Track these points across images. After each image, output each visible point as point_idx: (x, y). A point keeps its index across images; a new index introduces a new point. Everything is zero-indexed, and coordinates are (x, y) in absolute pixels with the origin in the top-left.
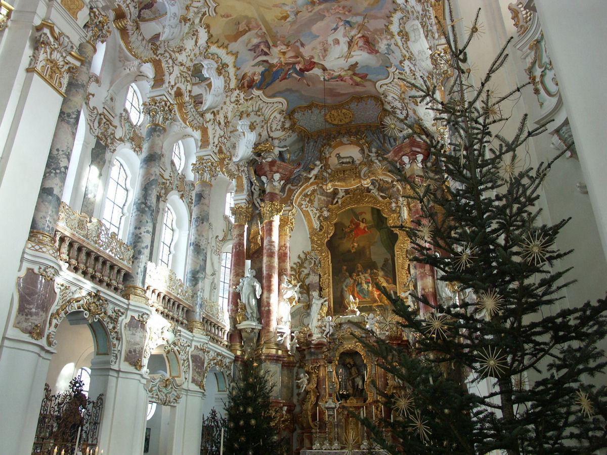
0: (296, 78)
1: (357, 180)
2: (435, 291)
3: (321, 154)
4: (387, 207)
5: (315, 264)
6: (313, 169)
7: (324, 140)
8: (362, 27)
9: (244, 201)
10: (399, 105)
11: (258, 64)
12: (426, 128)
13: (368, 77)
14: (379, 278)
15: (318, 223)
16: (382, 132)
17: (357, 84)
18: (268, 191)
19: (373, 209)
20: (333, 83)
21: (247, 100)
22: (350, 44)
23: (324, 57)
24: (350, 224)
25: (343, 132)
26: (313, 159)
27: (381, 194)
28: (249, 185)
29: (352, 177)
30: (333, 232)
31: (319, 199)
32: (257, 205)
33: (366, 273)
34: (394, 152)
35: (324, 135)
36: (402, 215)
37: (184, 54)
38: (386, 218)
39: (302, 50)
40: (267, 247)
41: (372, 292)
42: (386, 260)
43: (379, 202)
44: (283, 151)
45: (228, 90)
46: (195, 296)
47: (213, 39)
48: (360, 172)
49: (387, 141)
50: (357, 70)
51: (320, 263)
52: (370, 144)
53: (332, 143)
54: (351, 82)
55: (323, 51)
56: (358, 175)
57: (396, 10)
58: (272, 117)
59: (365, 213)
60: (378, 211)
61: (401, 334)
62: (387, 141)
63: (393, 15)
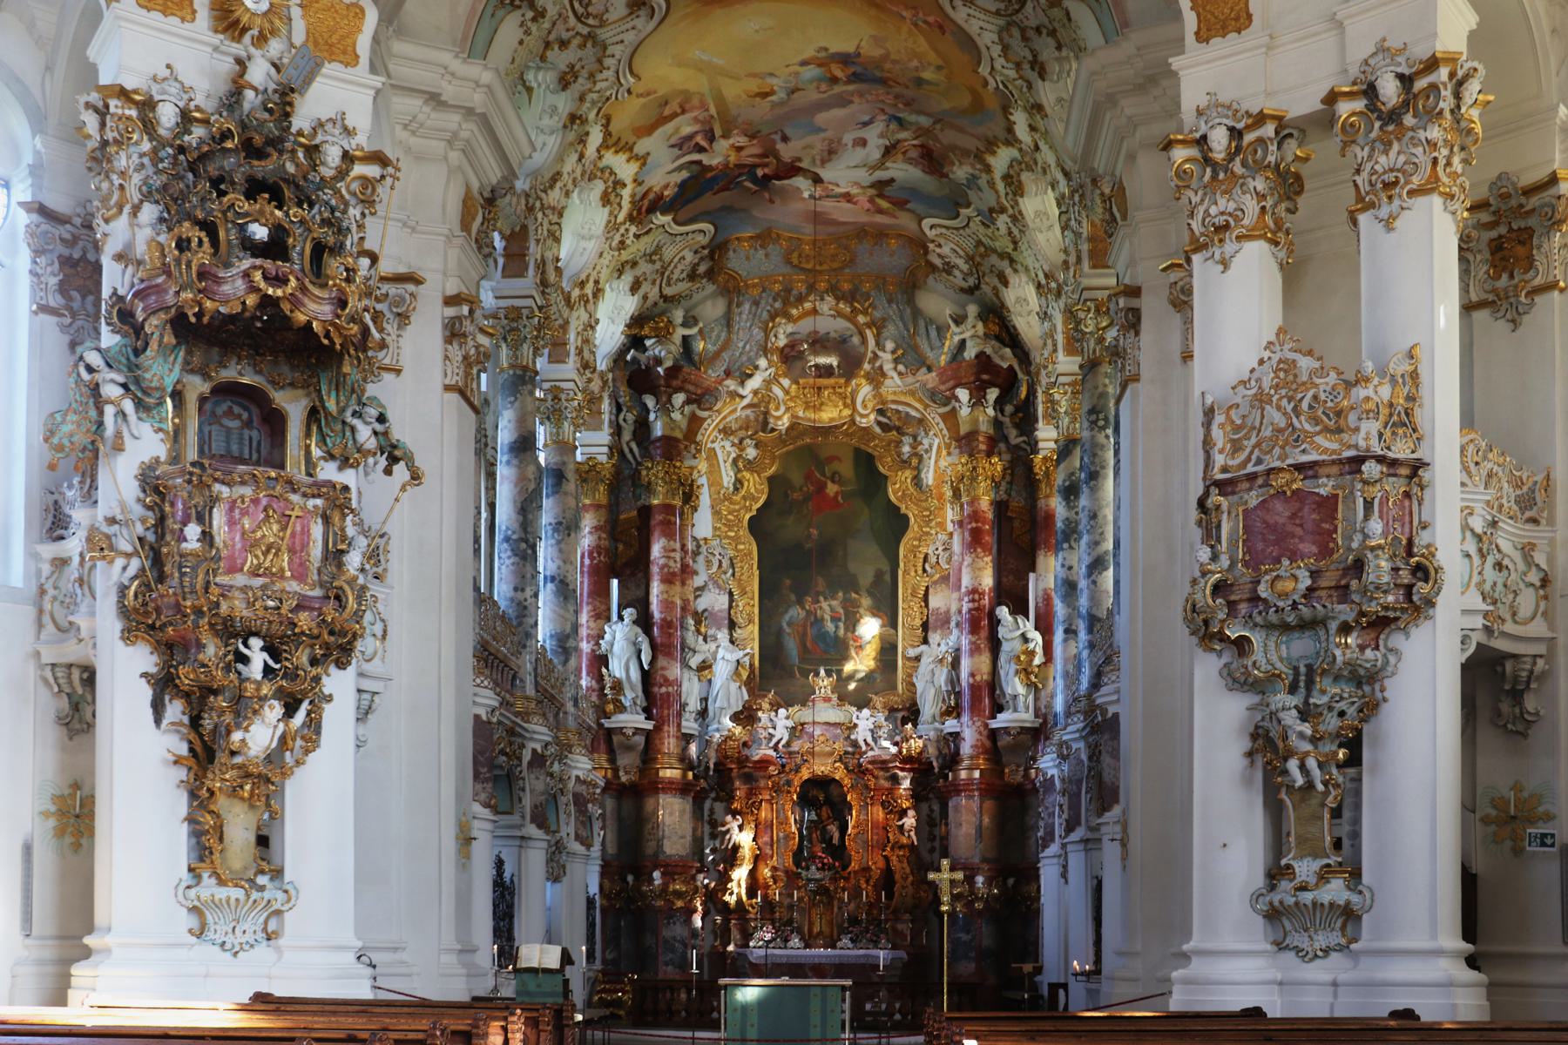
6: (750, 376)
7: (775, 300)
8: (921, 132)
10: (965, 267)
12: (1014, 327)
15: (732, 474)
16: (911, 301)
17: (880, 211)
18: (658, 430)
20: (827, 206)
21: (637, 236)
26: (748, 347)
29: (836, 406)
30: (764, 497)
33: (833, 598)
35: (777, 287)
36: (923, 475)
37: (559, 184)
38: (886, 478)
42: (879, 575)
45: (612, 226)
47: (610, 142)
49: (922, 330)
51: (732, 565)
52: (878, 326)
55: (826, 154)
56: (849, 401)
58: (676, 260)
60: (870, 459)
62: (922, 330)
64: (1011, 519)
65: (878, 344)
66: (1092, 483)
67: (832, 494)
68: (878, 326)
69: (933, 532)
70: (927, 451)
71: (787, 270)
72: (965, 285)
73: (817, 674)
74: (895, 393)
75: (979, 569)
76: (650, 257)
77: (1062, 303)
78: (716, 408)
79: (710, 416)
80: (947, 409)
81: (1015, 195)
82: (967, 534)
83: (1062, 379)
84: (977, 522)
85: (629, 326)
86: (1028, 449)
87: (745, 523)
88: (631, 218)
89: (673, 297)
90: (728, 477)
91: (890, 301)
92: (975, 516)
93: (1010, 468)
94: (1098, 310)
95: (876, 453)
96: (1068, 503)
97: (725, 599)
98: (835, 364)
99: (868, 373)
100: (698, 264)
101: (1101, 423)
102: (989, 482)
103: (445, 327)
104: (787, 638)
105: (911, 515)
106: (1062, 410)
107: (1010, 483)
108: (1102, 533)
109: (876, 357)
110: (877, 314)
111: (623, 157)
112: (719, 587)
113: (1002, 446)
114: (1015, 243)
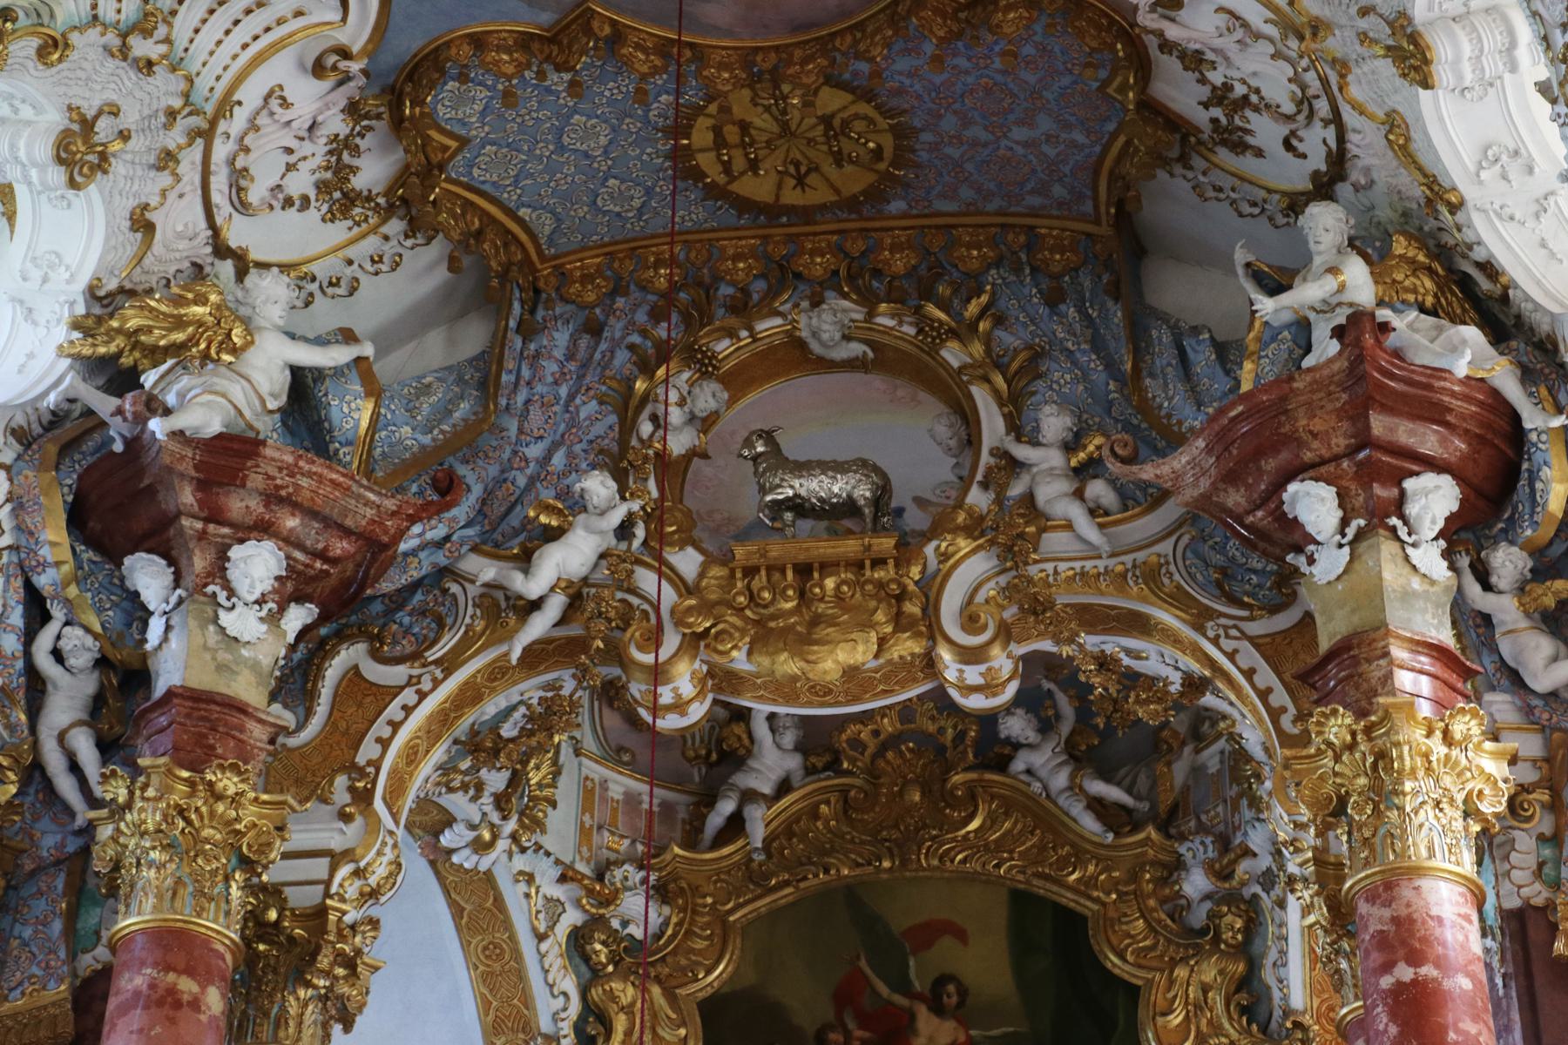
3: (627, 426)
4: (1139, 895)
15: (569, 984)
19: (1023, 903)
24: (827, 1012)
26: (558, 460)
27: (1098, 787)
29: (869, 625)
31: (590, 793)
32: (66, 786)
34: (1221, 441)
43: (1080, 852)
44: (319, 374)
48: (931, 590)
49: (1164, 357)
53: (723, 346)
56: (913, 608)
58: (251, 94)
59: (961, 935)
71: (694, 212)
78: (435, 654)
79: (411, 681)
109: (1014, 466)
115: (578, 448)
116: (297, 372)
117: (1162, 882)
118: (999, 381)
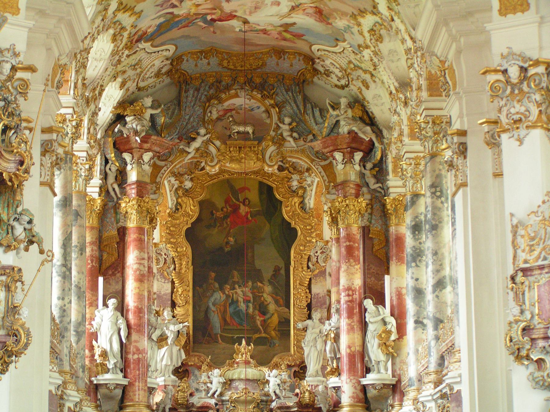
0: (200, 26)
1: (259, 164)
2: (363, 351)
3: (205, 113)
5: (165, 263)
6: (194, 139)
7: (210, 88)
9: (97, 190)
11: (160, 17)
12: (372, 113)
13: (304, 37)
14: (265, 295)
15: (175, 199)
17: (285, 39)
19: (261, 184)
21: (128, 56)
22: (293, 8)
23: (251, 13)
24: (223, 205)
25: (242, 80)
26: (192, 119)
28: (104, 163)
30: (196, 215)
32: (112, 193)
33: (245, 286)
35: (212, 80)
36: (306, 201)
38: (281, 202)
39: (225, 5)
40: (135, 266)
41: (253, 318)
42: (277, 270)
45: (113, 54)
46: (79, 356)
49: (309, 112)
50: (291, 29)
54: (277, 36)
57: (374, 14)
58: (149, 66)
59: (249, 190)
61: (314, 401)
62: (309, 112)
63: (368, 13)
64: (371, 238)
65: (279, 119)
66: (434, 232)
67: (243, 214)
68: (280, 106)
69: (314, 240)
70: (309, 186)
72: (339, 84)
73: (240, 344)
74: (291, 151)
75: (352, 274)
76: (134, 67)
77: (409, 110)
78: (170, 160)
79: (166, 165)
80: (327, 162)
81: (377, 40)
82: (343, 249)
83: (407, 155)
84: (350, 241)
85: (116, 108)
86: (383, 192)
87: (183, 233)
88: (127, 47)
89: (144, 87)
90: (170, 201)
91: (287, 91)
92: (349, 237)
93: (370, 205)
94: (434, 122)
95: (274, 186)
96: (414, 236)
97: (169, 285)
98: (251, 131)
99: (274, 138)
100: (162, 68)
101: (438, 194)
102: (357, 214)
103: (42, 145)
104: (212, 314)
105: (298, 229)
106: (409, 175)
107: (371, 214)
108: (441, 265)
109: (278, 127)
110: (279, 99)
111: (127, 14)
112: (165, 278)
113: (365, 189)
114: (375, 66)
115: (195, 117)
116: (151, 114)
117: (288, 181)
118: (277, 110)
